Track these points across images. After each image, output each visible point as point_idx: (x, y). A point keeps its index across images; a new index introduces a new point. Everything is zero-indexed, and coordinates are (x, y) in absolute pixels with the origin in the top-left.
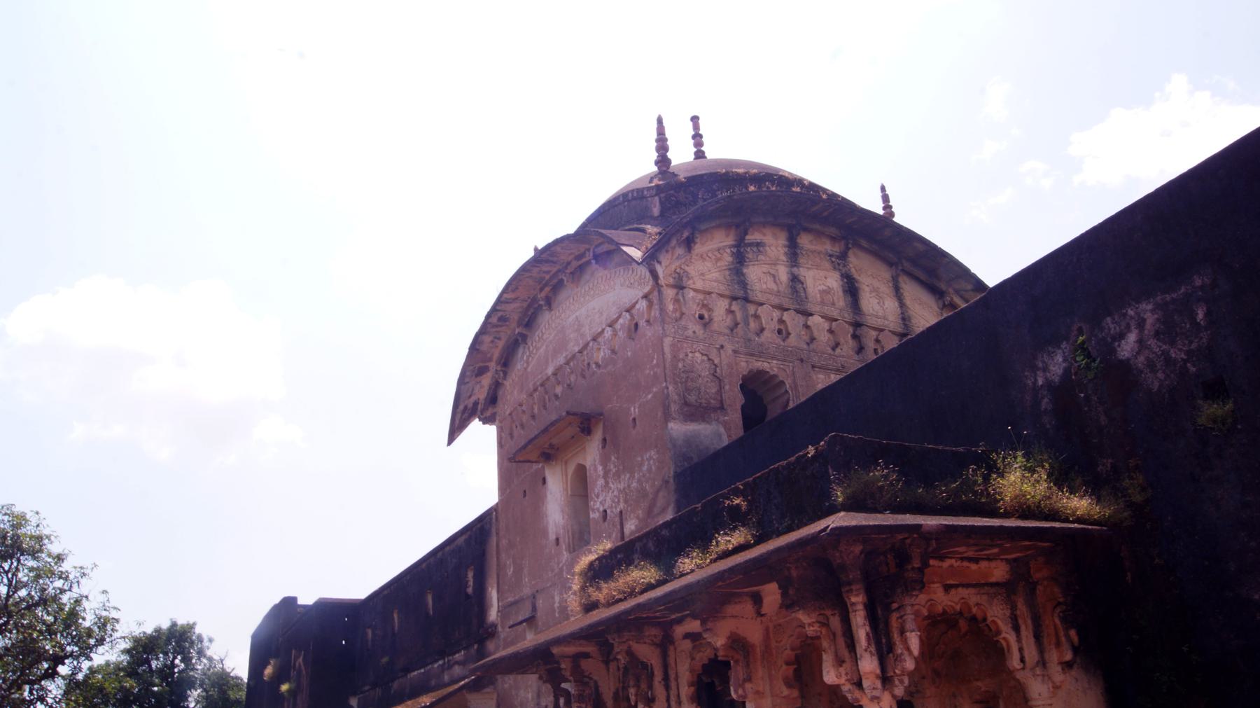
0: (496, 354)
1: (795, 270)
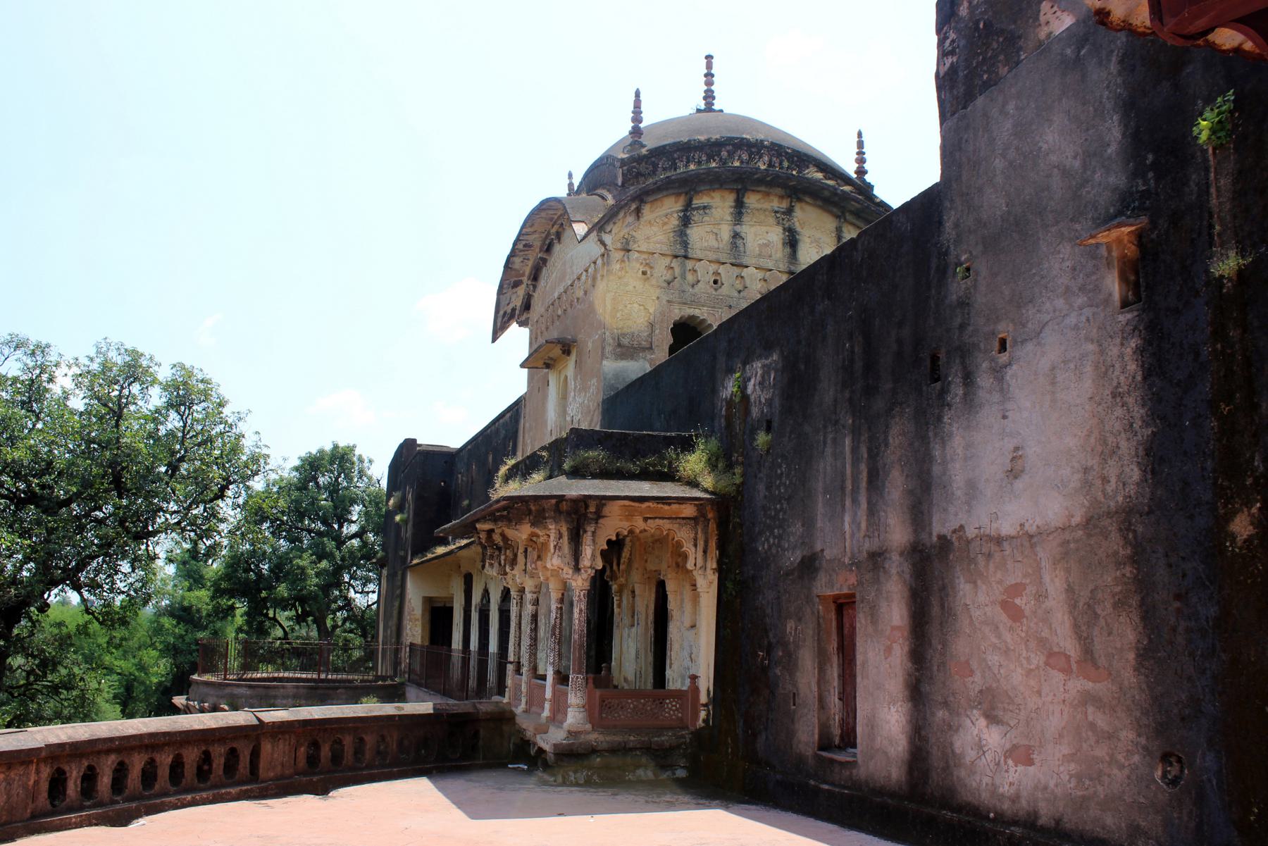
0: (528, 270)
1: (738, 228)
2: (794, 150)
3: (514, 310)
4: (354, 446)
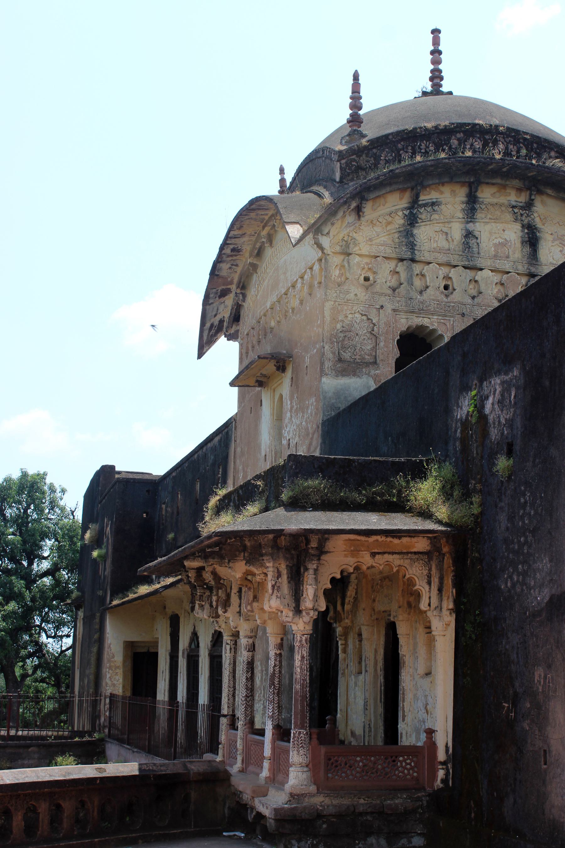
1: (471, 226)
2: (532, 136)
3: (221, 321)
4: (45, 474)
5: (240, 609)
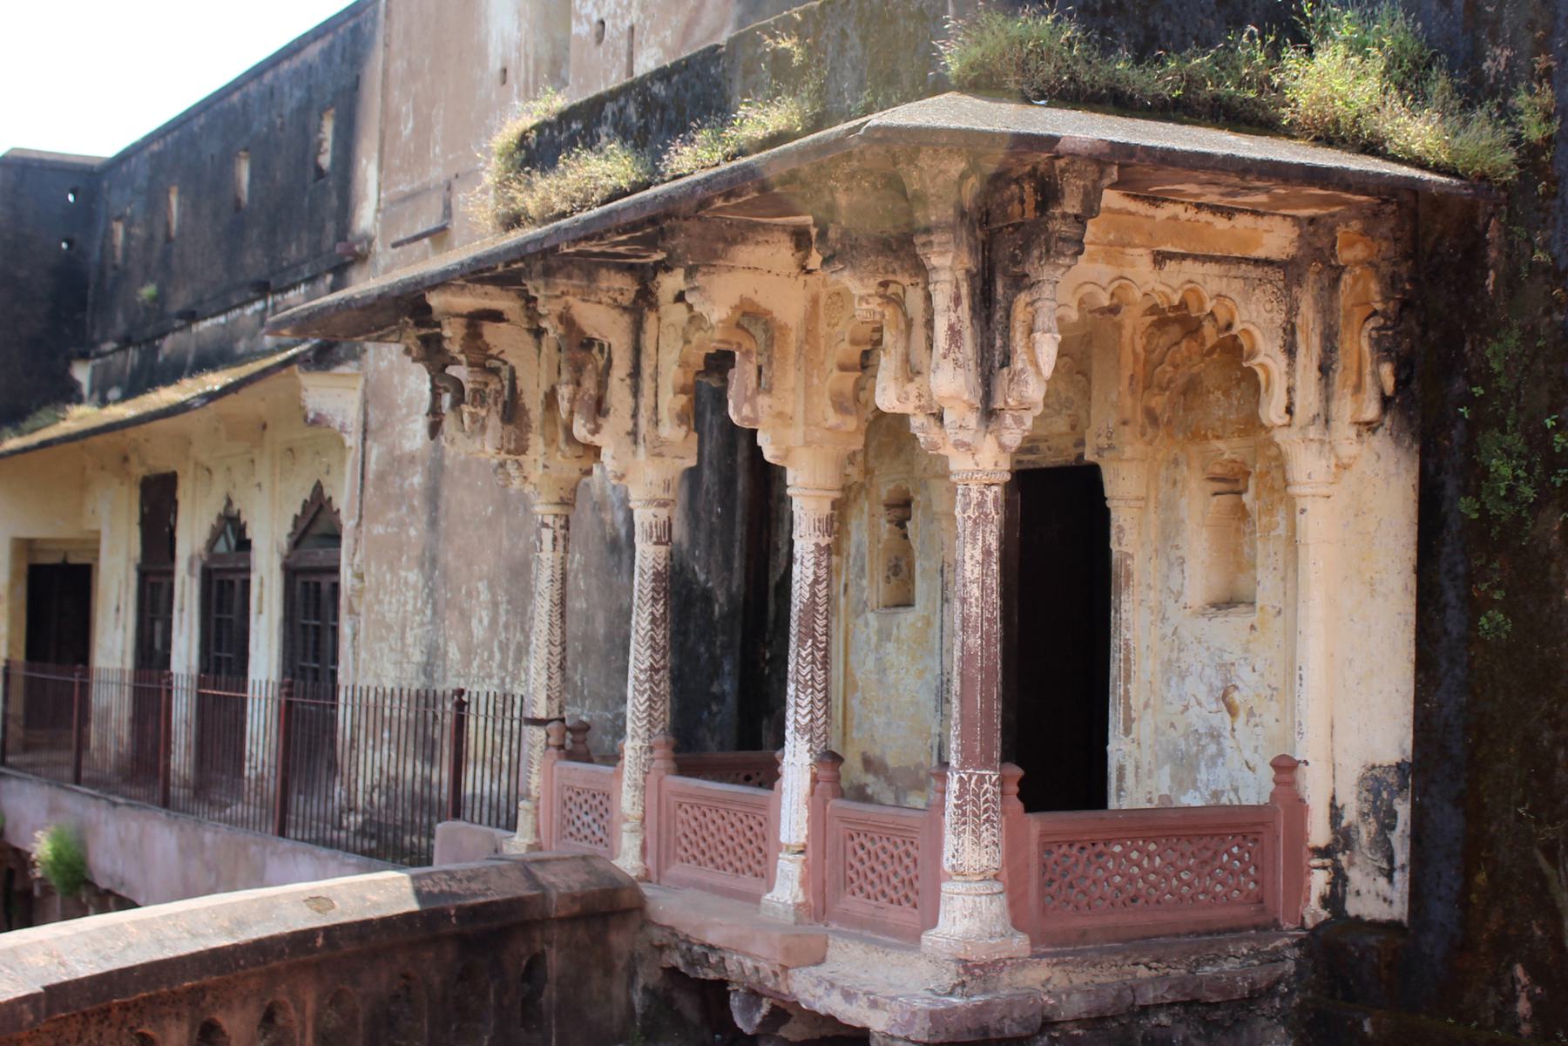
5: (636, 425)
